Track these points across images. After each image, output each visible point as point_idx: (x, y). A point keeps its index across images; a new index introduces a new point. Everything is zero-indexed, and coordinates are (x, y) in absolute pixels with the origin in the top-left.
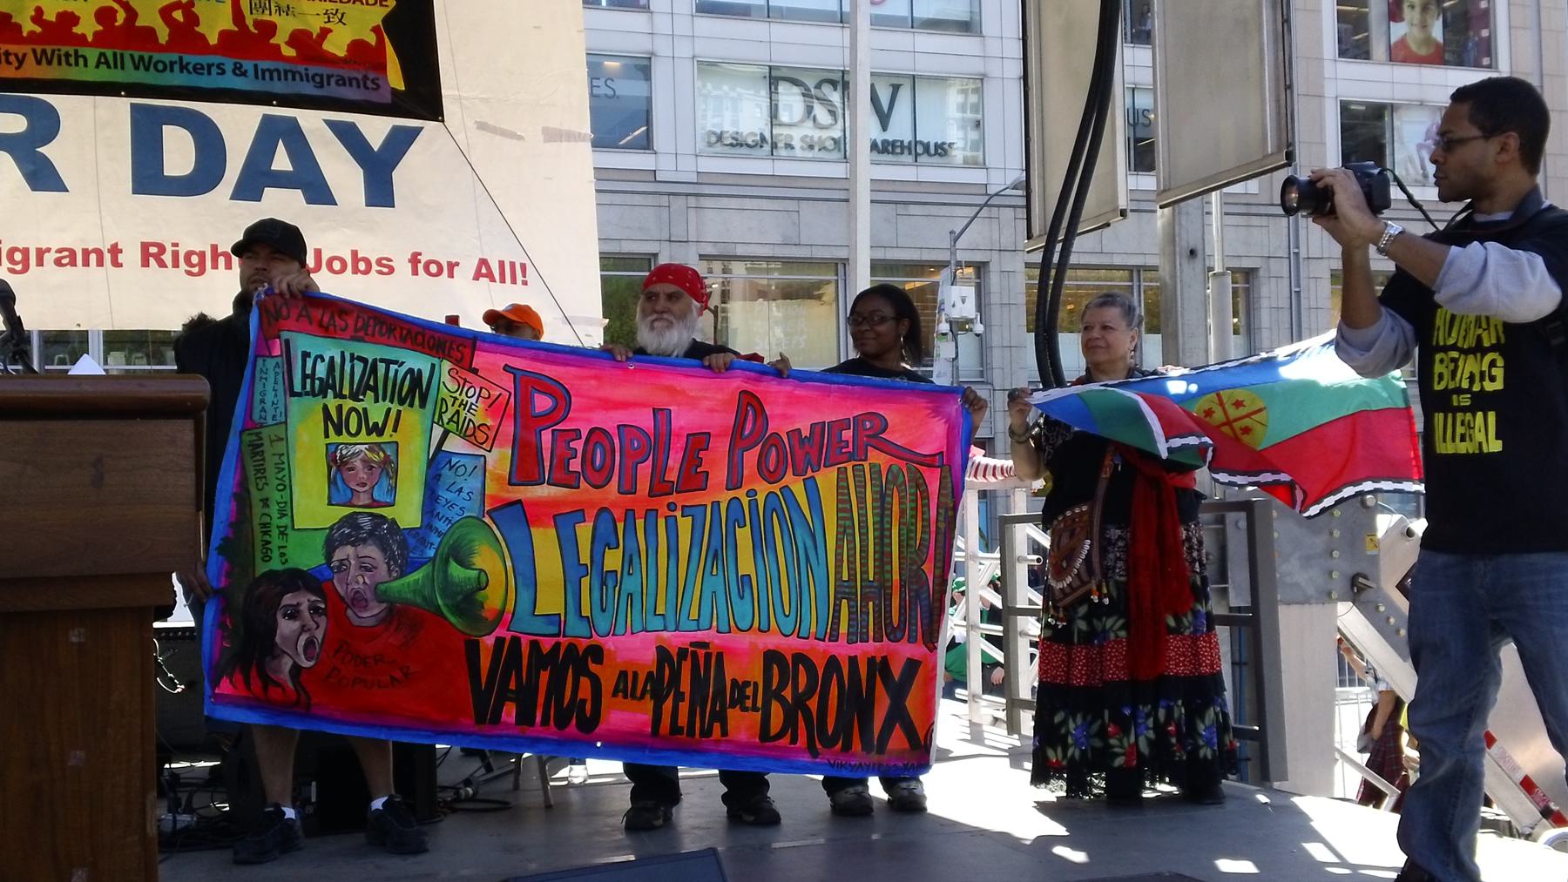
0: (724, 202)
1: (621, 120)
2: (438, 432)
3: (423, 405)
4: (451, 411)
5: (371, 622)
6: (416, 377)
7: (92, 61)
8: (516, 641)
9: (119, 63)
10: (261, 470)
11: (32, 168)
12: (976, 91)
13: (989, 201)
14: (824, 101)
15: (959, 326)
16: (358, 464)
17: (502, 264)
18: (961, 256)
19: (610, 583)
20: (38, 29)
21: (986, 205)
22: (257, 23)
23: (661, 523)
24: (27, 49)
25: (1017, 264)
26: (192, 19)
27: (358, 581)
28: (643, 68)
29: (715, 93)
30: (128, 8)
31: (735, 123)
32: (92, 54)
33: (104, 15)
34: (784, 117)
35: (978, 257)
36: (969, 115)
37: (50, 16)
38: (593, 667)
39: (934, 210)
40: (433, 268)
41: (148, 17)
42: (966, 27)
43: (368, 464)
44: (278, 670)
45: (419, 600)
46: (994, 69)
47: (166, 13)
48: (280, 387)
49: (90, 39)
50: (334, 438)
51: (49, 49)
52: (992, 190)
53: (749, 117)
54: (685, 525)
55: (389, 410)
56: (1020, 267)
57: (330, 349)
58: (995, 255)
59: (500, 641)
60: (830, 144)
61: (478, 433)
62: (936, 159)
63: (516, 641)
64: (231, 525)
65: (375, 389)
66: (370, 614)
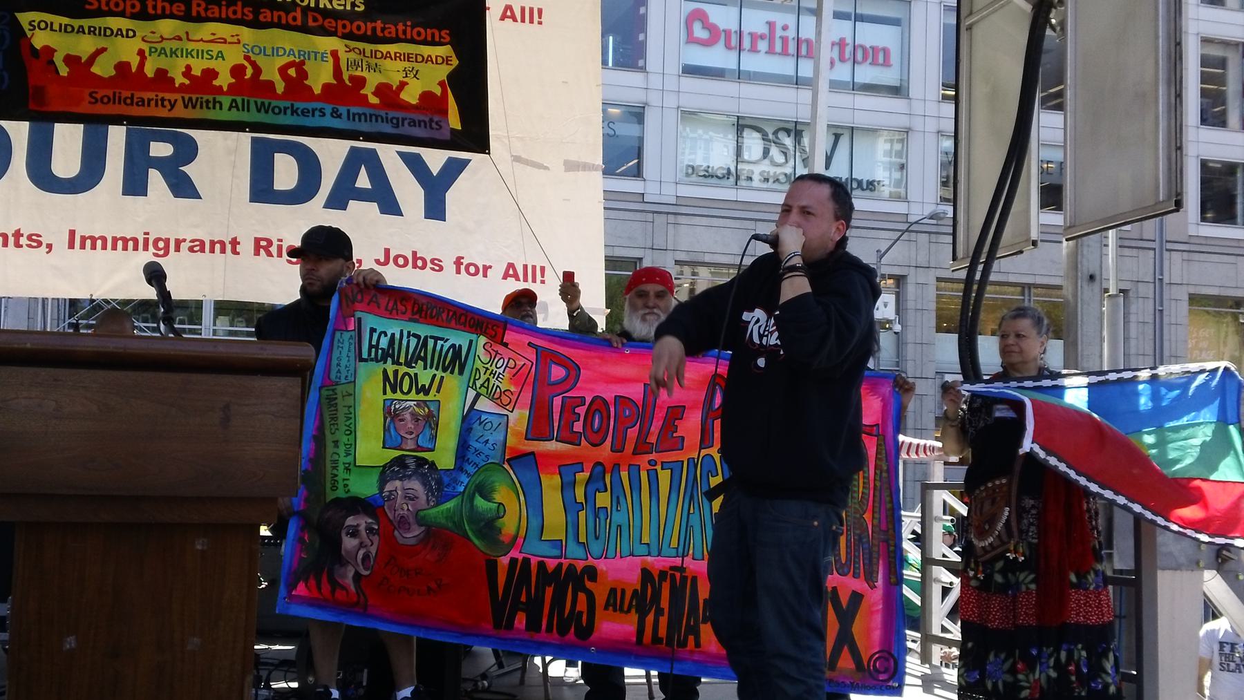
0: (697, 220)
1: (623, 156)
2: (472, 394)
3: (461, 373)
4: (483, 378)
5: (413, 542)
6: (457, 350)
7: (226, 105)
8: (526, 562)
9: (246, 107)
10: (334, 418)
12: (902, 141)
13: (909, 228)
14: (779, 144)
16: (408, 416)
17: (525, 267)
19: (602, 517)
20: (187, 82)
21: (907, 230)
22: (352, 78)
23: (644, 475)
24: (178, 96)
25: (930, 278)
26: (303, 74)
27: (404, 508)
28: (637, 114)
29: (691, 135)
30: (254, 64)
31: (706, 159)
32: (226, 100)
33: (237, 71)
34: (746, 156)
35: (897, 271)
36: (894, 159)
37: (197, 72)
38: (589, 584)
40: (472, 269)
41: (271, 72)
42: (896, 91)
43: (415, 417)
44: (344, 576)
45: (450, 525)
46: (917, 124)
47: (283, 71)
48: (352, 354)
49: (225, 89)
50: (390, 395)
51: (194, 97)
52: (912, 219)
53: (719, 154)
54: (664, 476)
55: (434, 376)
57: (394, 327)
59: (513, 561)
60: (782, 178)
61: (504, 398)
62: (867, 193)
63: (526, 562)
64: (310, 460)
65: (424, 359)
66: (412, 535)
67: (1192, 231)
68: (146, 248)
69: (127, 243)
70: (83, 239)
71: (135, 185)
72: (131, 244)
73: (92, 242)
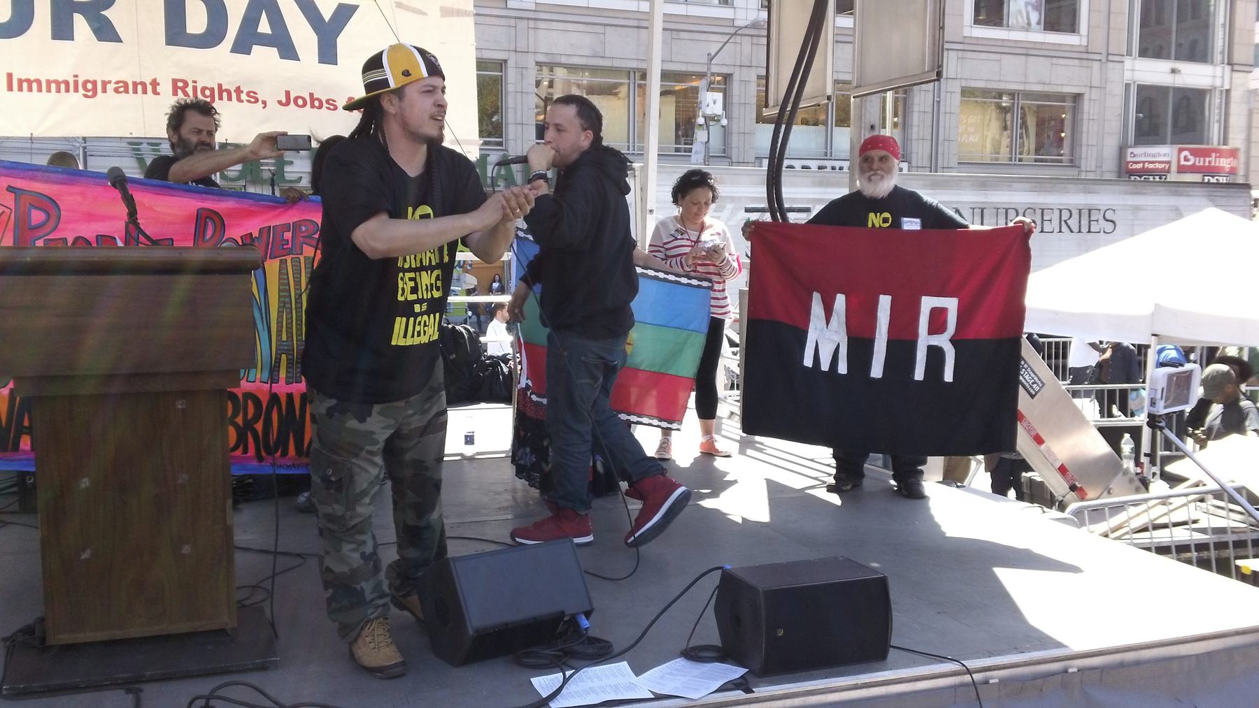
11: (97, 25)
13: (736, 32)
15: (710, 119)
18: (715, 69)
21: (735, 34)
25: (752, 75)
35: (725, 70)
39: (697, 36)
52: (737, 23)
56: (754, 78)
58: (738, 69)
67: (967, 32)
68: (76, 90)
69: (63, 86)
70: (20, 82)
71: (62, 30)
72: (63, 86)
73: (28, 84)
